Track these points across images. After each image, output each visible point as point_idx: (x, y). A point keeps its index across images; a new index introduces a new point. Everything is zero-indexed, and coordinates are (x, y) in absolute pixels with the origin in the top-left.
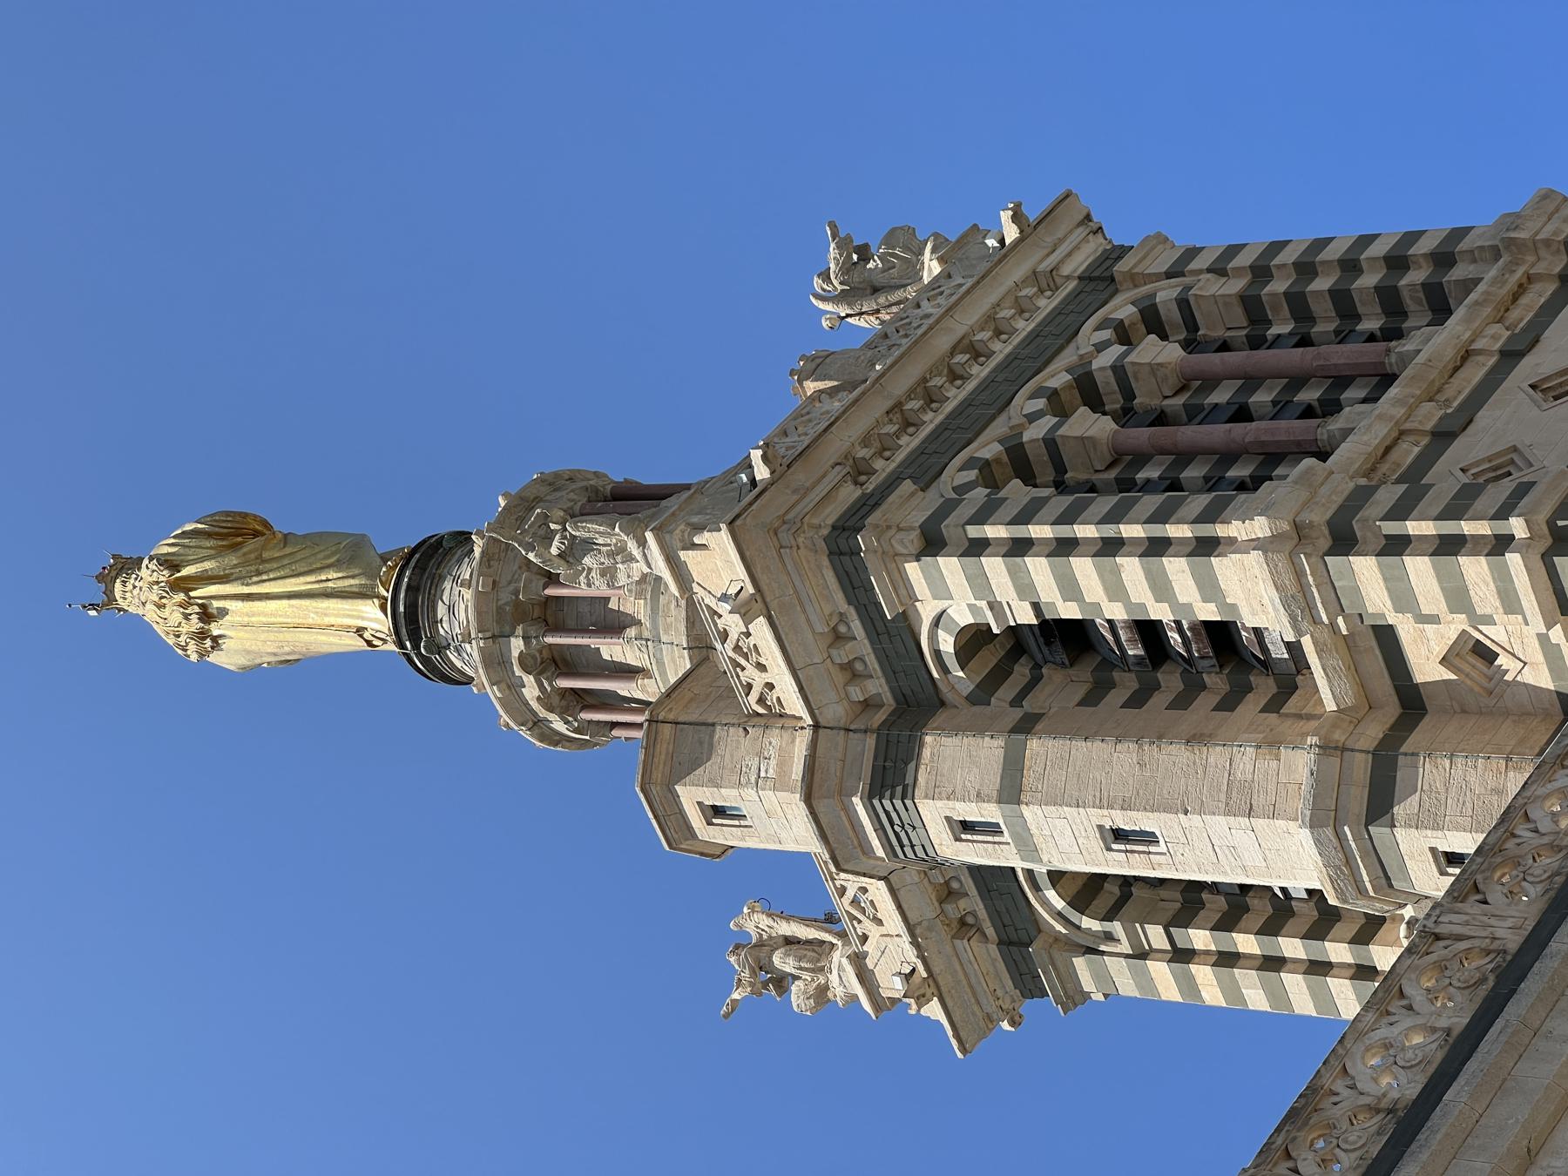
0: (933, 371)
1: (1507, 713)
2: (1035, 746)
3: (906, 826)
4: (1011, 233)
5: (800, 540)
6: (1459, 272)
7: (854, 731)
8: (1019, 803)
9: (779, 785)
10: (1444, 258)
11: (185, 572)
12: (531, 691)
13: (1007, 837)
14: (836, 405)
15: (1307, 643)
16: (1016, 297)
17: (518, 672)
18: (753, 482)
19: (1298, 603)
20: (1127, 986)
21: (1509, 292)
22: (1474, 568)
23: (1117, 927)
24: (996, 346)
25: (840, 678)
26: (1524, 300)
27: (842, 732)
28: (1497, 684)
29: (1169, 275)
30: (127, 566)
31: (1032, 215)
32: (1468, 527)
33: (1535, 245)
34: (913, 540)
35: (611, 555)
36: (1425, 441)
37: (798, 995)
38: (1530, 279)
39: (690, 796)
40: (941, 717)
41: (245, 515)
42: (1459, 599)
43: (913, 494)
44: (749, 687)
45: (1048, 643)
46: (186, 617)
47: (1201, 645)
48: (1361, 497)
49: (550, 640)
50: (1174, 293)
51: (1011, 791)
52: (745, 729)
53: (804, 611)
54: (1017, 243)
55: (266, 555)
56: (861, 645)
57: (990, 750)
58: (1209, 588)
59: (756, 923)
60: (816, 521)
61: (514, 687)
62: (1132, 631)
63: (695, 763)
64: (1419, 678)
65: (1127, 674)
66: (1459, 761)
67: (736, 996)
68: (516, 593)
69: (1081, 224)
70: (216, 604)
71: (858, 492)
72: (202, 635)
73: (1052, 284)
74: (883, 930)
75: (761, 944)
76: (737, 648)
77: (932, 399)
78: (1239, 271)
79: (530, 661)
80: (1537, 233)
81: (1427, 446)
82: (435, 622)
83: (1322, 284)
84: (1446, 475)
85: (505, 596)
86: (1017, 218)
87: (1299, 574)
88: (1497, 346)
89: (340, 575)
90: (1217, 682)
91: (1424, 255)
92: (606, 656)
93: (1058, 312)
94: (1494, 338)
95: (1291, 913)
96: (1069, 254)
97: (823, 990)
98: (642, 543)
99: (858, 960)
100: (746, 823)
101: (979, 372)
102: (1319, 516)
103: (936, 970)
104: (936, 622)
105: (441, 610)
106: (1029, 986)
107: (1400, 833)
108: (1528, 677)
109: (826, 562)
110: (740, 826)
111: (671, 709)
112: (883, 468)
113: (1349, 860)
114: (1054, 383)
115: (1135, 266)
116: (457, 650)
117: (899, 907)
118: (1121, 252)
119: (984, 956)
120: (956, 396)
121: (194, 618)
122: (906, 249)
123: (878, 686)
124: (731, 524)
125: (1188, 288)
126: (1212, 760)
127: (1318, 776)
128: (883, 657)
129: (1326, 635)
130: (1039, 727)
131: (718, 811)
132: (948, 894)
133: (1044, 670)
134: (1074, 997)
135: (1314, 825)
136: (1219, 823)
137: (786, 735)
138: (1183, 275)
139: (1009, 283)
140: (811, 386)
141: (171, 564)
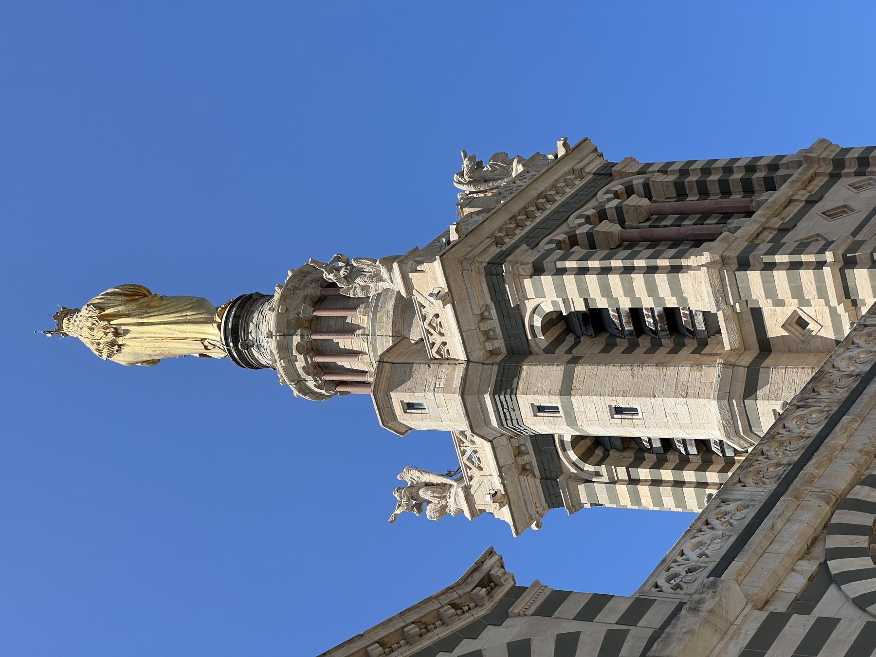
0: (530, 204)
1: (810, 352)
2: (579, 370)
3: (510, 409)
4: (561, 152)
5: (473, 267)
6: (781, 172)
7: (486, 364)
9: (447, 390)
10: (774, 166)
11: (107, 312)
12: (300, 363)
13: (561, 413)
14: (480, 219)
15: (720, 315)
16: (565, 179)
17: (295, 353)
18: (449, 242)
19: (720, 295)
20: (603, 498)
21: (807, 179)
22: (807, 276)
23: (603, 469)
24: (557, 198)
25: (482, 338)
26: (814, 183)
27: (481, 364)
28: (810, 337)
29: (638, 173)
30: (70, 312)
31: (572, 145)
32: (804, 258)
33: (819, 160)
34: (529, 269)
35: (371, 277)
36: (775, 232)
37: (430, 512)
38: (816, 175)
39: (397, 398)
40: (530, 358)
41: (140, 286)
42: (797, 292)
43: (527, 250)
44: (434, 344)
45: (585, 325)
46: (106, 334)
47: (662, 324)
48: (752, 245)
49: (314, 337)
50: (642, 181)
51: (566, 390)
52: (429, 365)
53: (470, 303)
54: (563, 157)
55: (152, 304)
56: (494, 323)
57: (556, 372)
58: (676, 289)
59: (411, 476)
60: (480, 260)
61: (290, 361)
62: (629, 318)
63: (402, 382)
64: (770, 335)
65: (624, 340)
66: (789, 370)
67: (398, 512)
68: (299, 314)
69: (593, 152)
70: (123, 327)
71: (499, 250)
72: (112, 344)
73: (581, 176)
74: (482, 473)
75: (412, 486)
76: (430, 325)
77: (529, 216)
78: (673, 172)
79: (301, 349)
80: (820, 155)
81: (776, 234)
82: (247, 333)
83: (714, 177)
84: (791, 239)
85: (292, 316)
86: (565, 145)
87: (722, 280)
88: (804, 198)
89: (194, 313)
90: (668, 342)
91: (763, 165)
92: (341, 346)
93: (585, 186)
94: (803, 196)
95: (688, 461)
96: (589, 163)
97: (444, 508)
98: (390, 270)
99: (467, 490)
100: (425, 411)
101: (550, 208)
102: (733, 254)
103: (509, 490)
104: (534, 311)
105: (252, 327)
106: (553, 500)
107: (760, 403)
108: (823, 333)
109: (484, 279)
110: (421, 413)
111: (389, 357)
112: (509, 242)
113: (733, 417)
114: (616, 188)
115: (621, 169)
116: (258, 347)
117: (496, 457)
119: (533, 485)
120: (540, 216)
121: (111, 335)
122: (503, 162)
123: (500, 344)
124: (441, 257)
125: (648, 179)
126: (668, 373)
127: (722, 378)
128: (504, 328)
129: (729, 312)
130: (580, 361)
131: (410, 406)
132: (519, 452)
133: (582, 338)
134: (576, 506)
135: (719, 398)
136: (670, 401)
137: (451, 367)
138: (645, 173)
139: (562, 172)
140: (467, 211)
141: (100, 308)
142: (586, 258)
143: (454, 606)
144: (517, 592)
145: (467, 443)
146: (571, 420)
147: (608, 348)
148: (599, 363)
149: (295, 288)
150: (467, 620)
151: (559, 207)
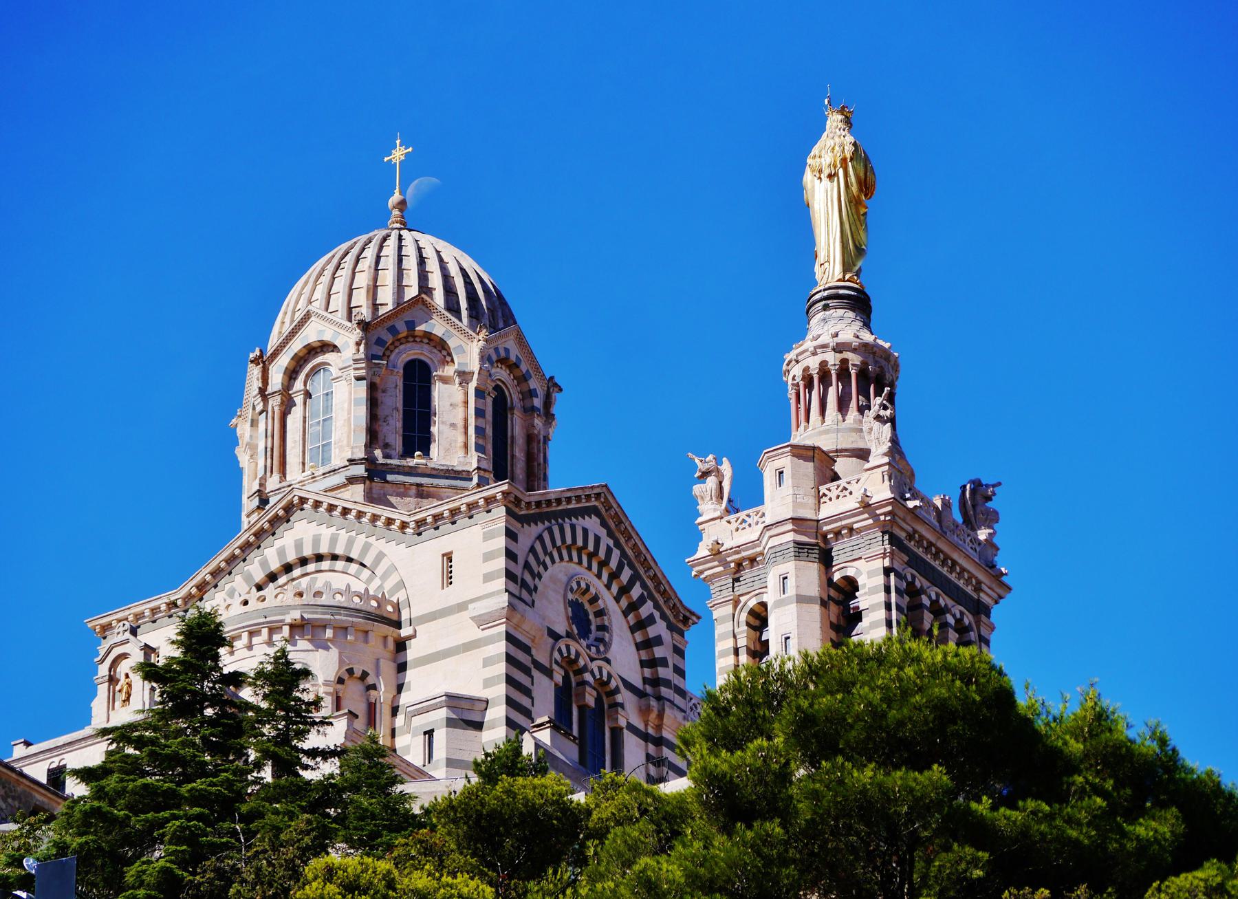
2: (816, 609)
8: (797, 602)
9: (796, 504)
13: (783, 596)
29: (980, 636)
50: (973, 639)
51: (801, 599)
70: (836, 179)
74: (734, 531)
75: (718, 470)
79: (824, 364)
105: (841, 312)
112: (911, 545)
118: (988, 615)
137: (813, 506)
142: (899, 608)
143: (674, 605)
144: (682, 634)
145: (756, 518)
146: (779, 604)
147: (833, 626)
148: (822, 622)
149: (874, 353)
150: (668, 612)
151: (946, 578)
